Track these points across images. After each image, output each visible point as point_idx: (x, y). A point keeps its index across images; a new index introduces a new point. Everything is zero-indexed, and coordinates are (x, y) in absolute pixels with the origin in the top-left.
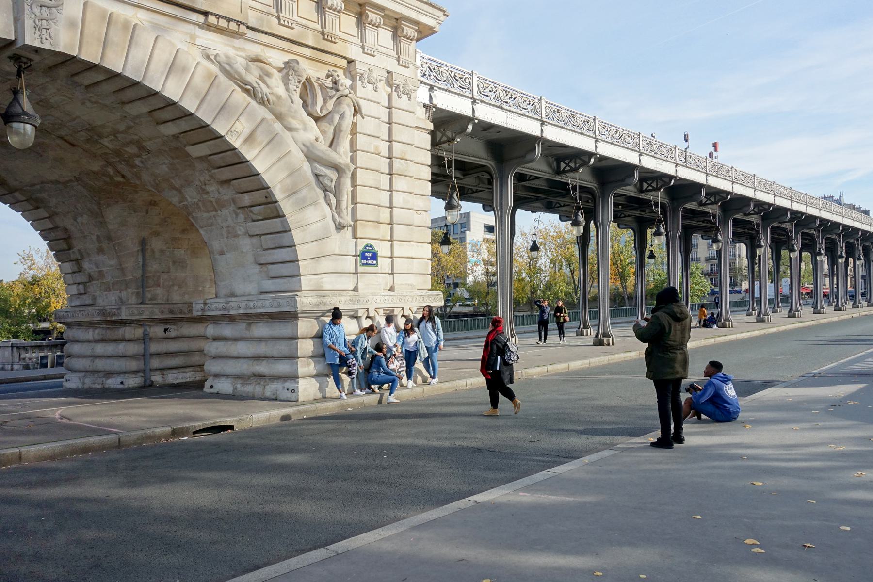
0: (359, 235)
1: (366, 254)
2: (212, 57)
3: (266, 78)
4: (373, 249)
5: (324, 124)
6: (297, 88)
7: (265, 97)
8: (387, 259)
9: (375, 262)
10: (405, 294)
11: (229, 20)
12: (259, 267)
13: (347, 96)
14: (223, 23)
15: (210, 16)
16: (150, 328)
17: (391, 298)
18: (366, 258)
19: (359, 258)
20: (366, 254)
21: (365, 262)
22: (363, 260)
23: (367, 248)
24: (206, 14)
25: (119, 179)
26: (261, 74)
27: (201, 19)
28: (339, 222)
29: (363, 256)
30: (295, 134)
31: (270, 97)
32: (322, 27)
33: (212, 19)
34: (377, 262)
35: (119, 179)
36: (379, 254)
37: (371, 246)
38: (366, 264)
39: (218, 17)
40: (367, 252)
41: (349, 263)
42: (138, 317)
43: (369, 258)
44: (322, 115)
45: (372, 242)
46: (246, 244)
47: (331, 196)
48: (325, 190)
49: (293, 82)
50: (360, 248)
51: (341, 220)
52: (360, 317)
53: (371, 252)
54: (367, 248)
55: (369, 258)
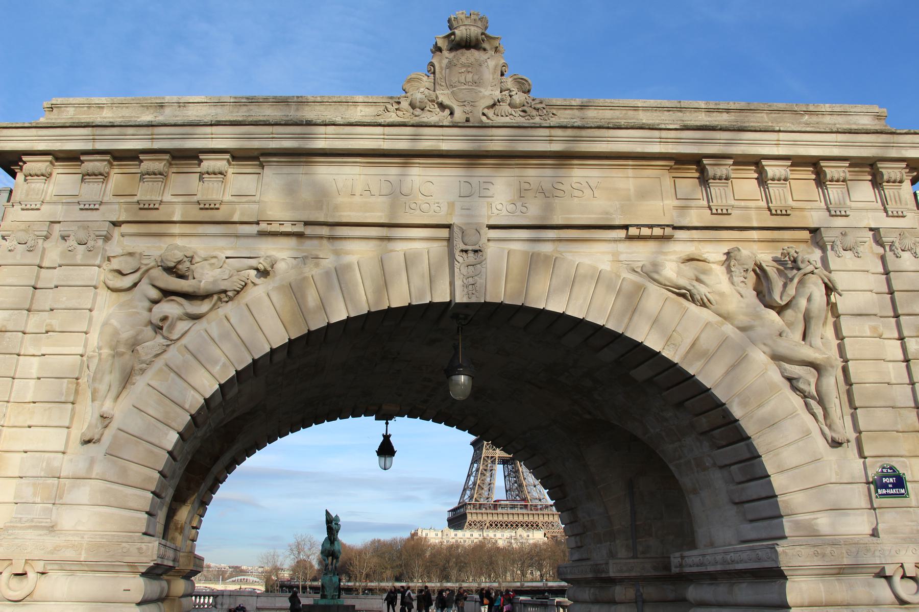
2: (639, 270)
3: (702, 277)
4: (894, 471)
5: (789, 313)
6: (745, 278)
7: (705, 298)
9: (903, 491)
11: (651, 227)
12: (735, 507)
13: (812, 273)
14: (646, 232)
15: (630, 229)
16: (643, 588)
18: (885, 486)
19: (872, 486)
20: (884, 480)
21: (884, 491)
22: (881, 488)
24: (626, 227)
25: (588, 417)
26: (696, 273)
27: (622, 234)
29: (879, 484)
30: (751, 333)
31: (709, 296)
32: (768, 203)
33: (633, 231)
34: (907, 491)
35: (588, 417)
36: (908, 477)
38: (887, 494)
39: (639, 226)
40: (886, 477)
41: (858, 496)
42: (626, 574)
43: (890, 486)
44: (783, 303)
45: (894, 462)
46: (717, 478)
47: (813, 403)
48: (805, 396)
49: (737, 273)
50: (873, 473)
51: (834, 435)
52: (891, 577)
55: (890, 486)
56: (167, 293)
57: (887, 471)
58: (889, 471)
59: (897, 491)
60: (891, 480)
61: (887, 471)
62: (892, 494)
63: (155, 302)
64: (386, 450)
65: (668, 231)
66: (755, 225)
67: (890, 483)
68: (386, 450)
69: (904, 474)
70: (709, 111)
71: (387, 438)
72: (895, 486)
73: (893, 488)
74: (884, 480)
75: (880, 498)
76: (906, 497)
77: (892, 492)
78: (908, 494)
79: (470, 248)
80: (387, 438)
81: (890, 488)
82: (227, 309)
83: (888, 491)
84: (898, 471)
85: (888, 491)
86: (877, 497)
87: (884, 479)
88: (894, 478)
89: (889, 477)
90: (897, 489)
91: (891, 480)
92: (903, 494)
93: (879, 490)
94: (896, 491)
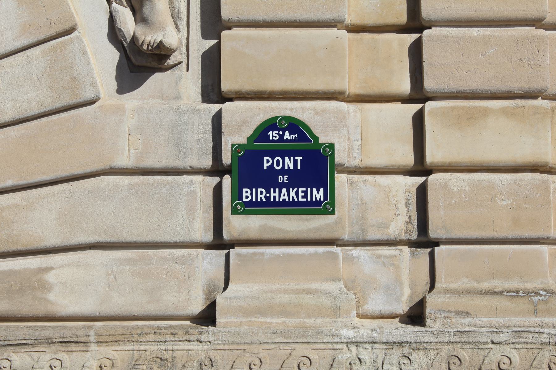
0: (226, 86)
1: (267, 162)
4: (303, 137)
8: (401, 179)
9: (318, 195)
10: (488, 338)
17: (395, 354)
19: (227, 181)
20: (267, 162)
21: (261, 194)
23: (274, 135)
28: (134, 39)
34: (330, 195)
36: (340, 157)
38: (268, 202)
53: (292, 153)
54: (274, 135)
55: (280, 179)
57: (281, 137)
58: (287, 136)
59: (301, 194)
60: (289, 163)
61: (281, 137)
62: (284, 203)
67: (283, 172)
69: (331, 146)
73: (288, 186)
75: (245, 213)
76: (325, 212)
77: (284, 196)
78: (332, 203)
81: (281, 186)
83: (273, 194)
84: (316, 139)
85: (273, 194)
86: (235, 212)
87: (266, 159)
88: (299, 159)
89: (283, 154)
90: (301, 190)
91: (289, 163)
92: (318, 203)
93: (245, 190)
94: (297, 193)
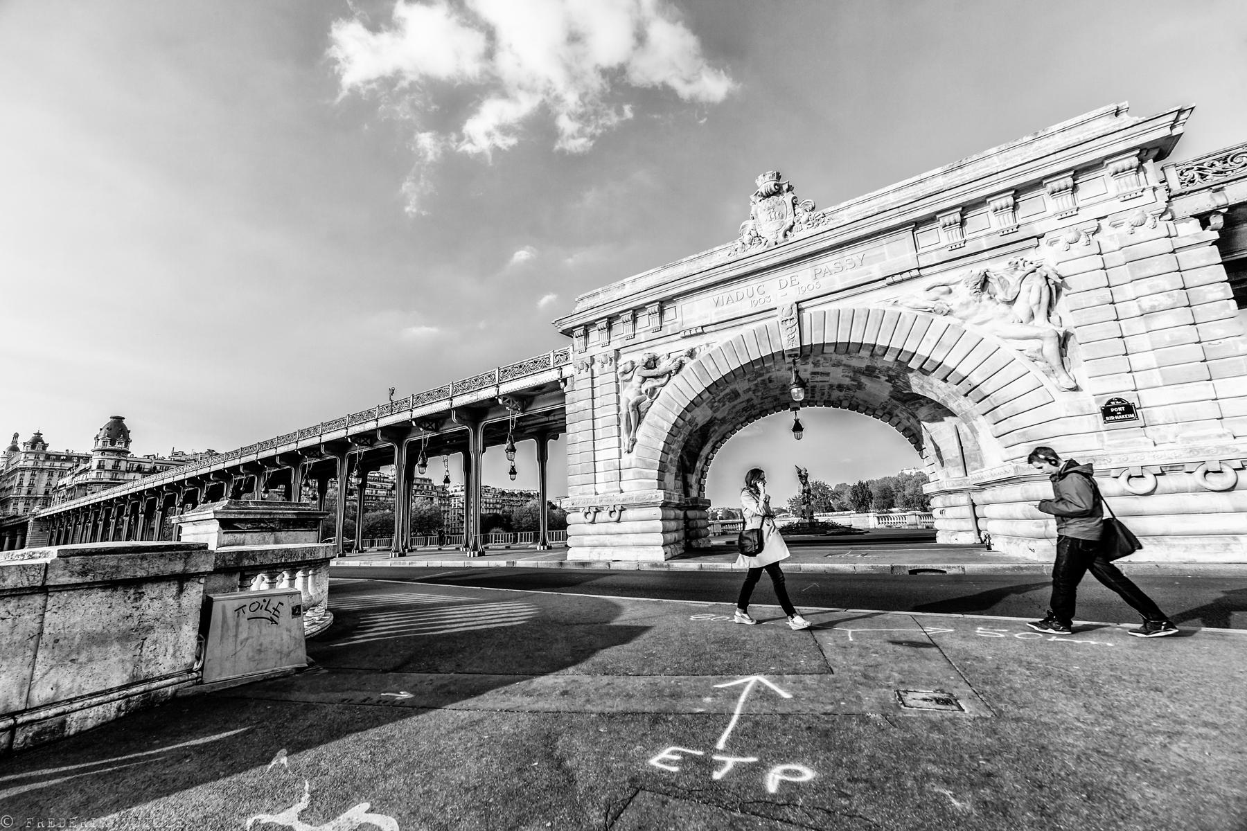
9: (1133, 416)
18: (1114, 414)
21: (1112, 418)
23: (1112, 403)
37: (1119, 400)
40: (1114, 407)
56: (645, 379)
63: (643, 382)
64: (798, 428)
65: (915, 273)
66: (986, 248)
68: (798, 428)
70: (946, 173)
71: (797, 421)
72: (1123, 413)
74: (1112, 410)
79: (788, 318)
80: (797, 421)
82: (676, 379)
85: (1116, 417)
89: (1117, 407)
91: (1120, 409)
